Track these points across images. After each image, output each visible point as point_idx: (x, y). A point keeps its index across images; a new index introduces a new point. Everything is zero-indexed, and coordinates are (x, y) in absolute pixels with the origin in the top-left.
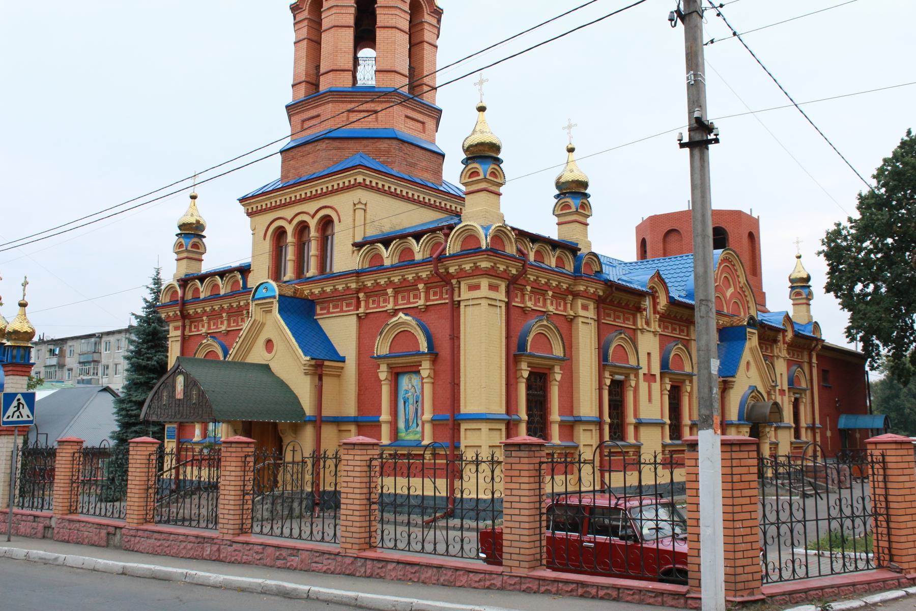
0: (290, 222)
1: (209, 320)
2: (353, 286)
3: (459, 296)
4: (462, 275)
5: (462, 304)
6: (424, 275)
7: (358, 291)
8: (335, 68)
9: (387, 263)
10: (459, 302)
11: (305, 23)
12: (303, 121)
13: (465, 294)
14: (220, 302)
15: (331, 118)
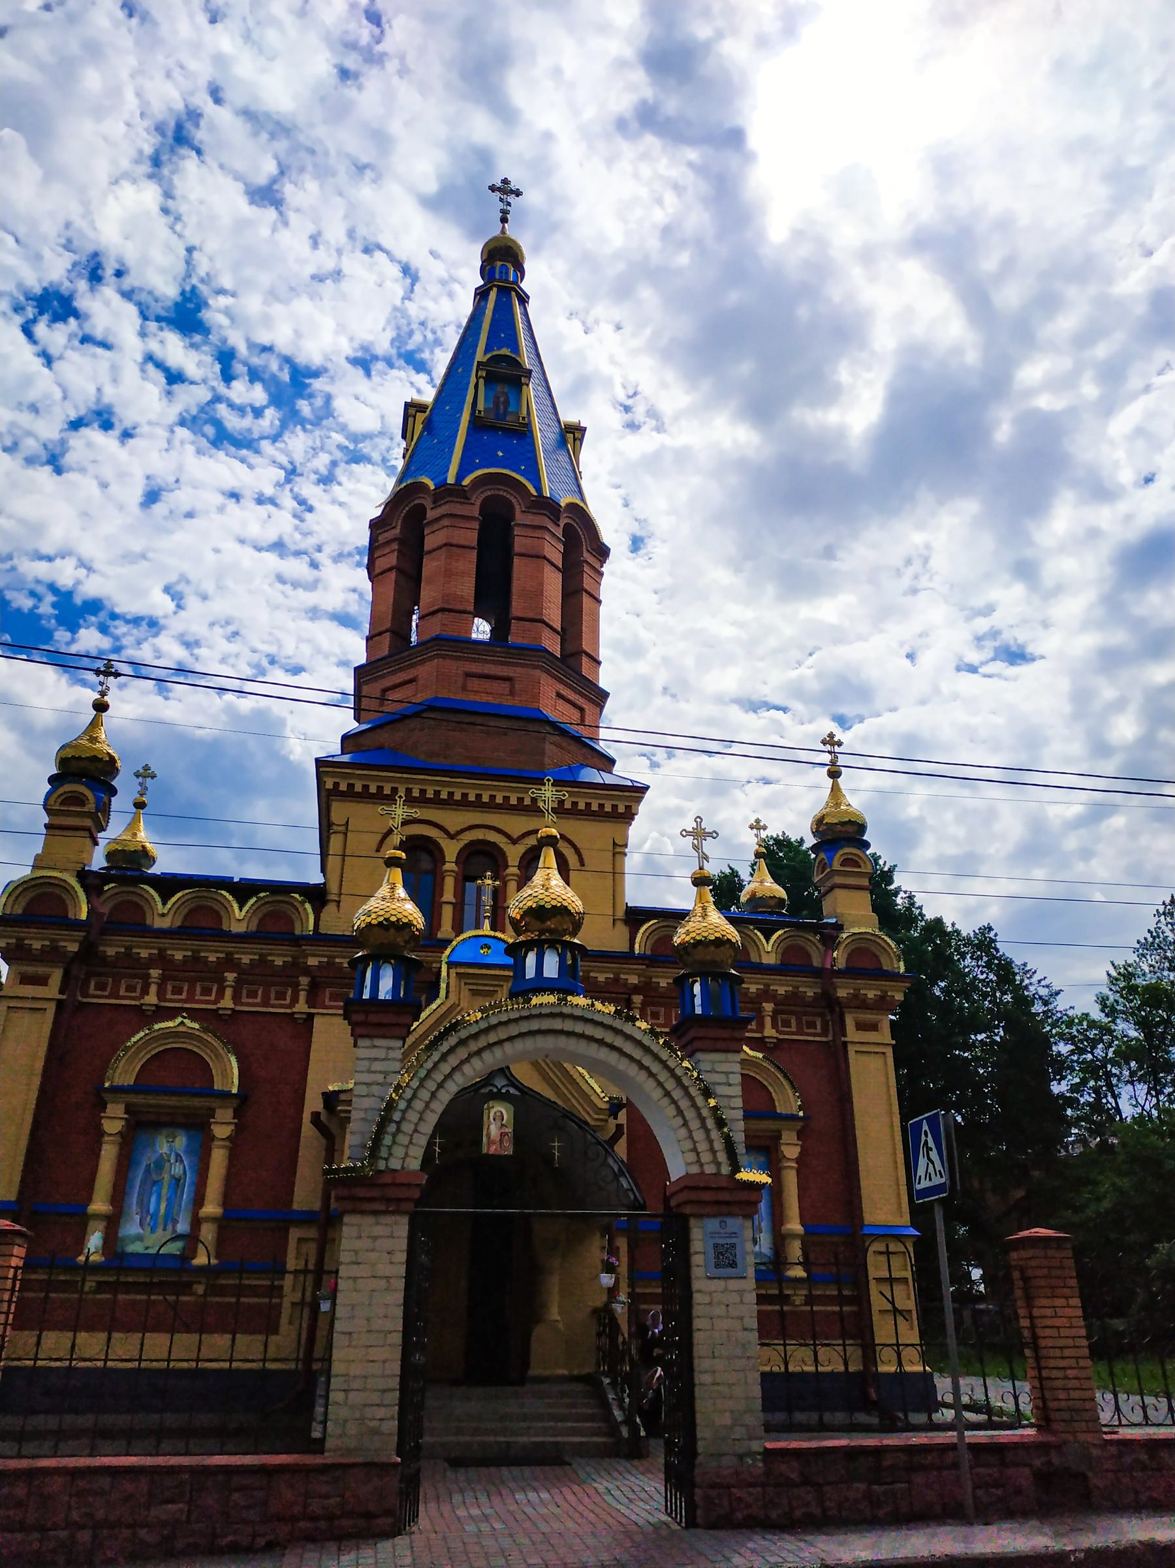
0: (452, 837)
1: (163, 980)
2: (633, 980)
3: (845, 1036)
4: (861, 1004)
5: (851, 1049)
6: (781, 990)
7: (636, 989)
8: (446, 606)
9: (238, 928)
10: (845, 1044)
11: (476, 525)
12: (468, 675)
13: (852, 1034)
14: (230, 947)
15: (430, 680)
